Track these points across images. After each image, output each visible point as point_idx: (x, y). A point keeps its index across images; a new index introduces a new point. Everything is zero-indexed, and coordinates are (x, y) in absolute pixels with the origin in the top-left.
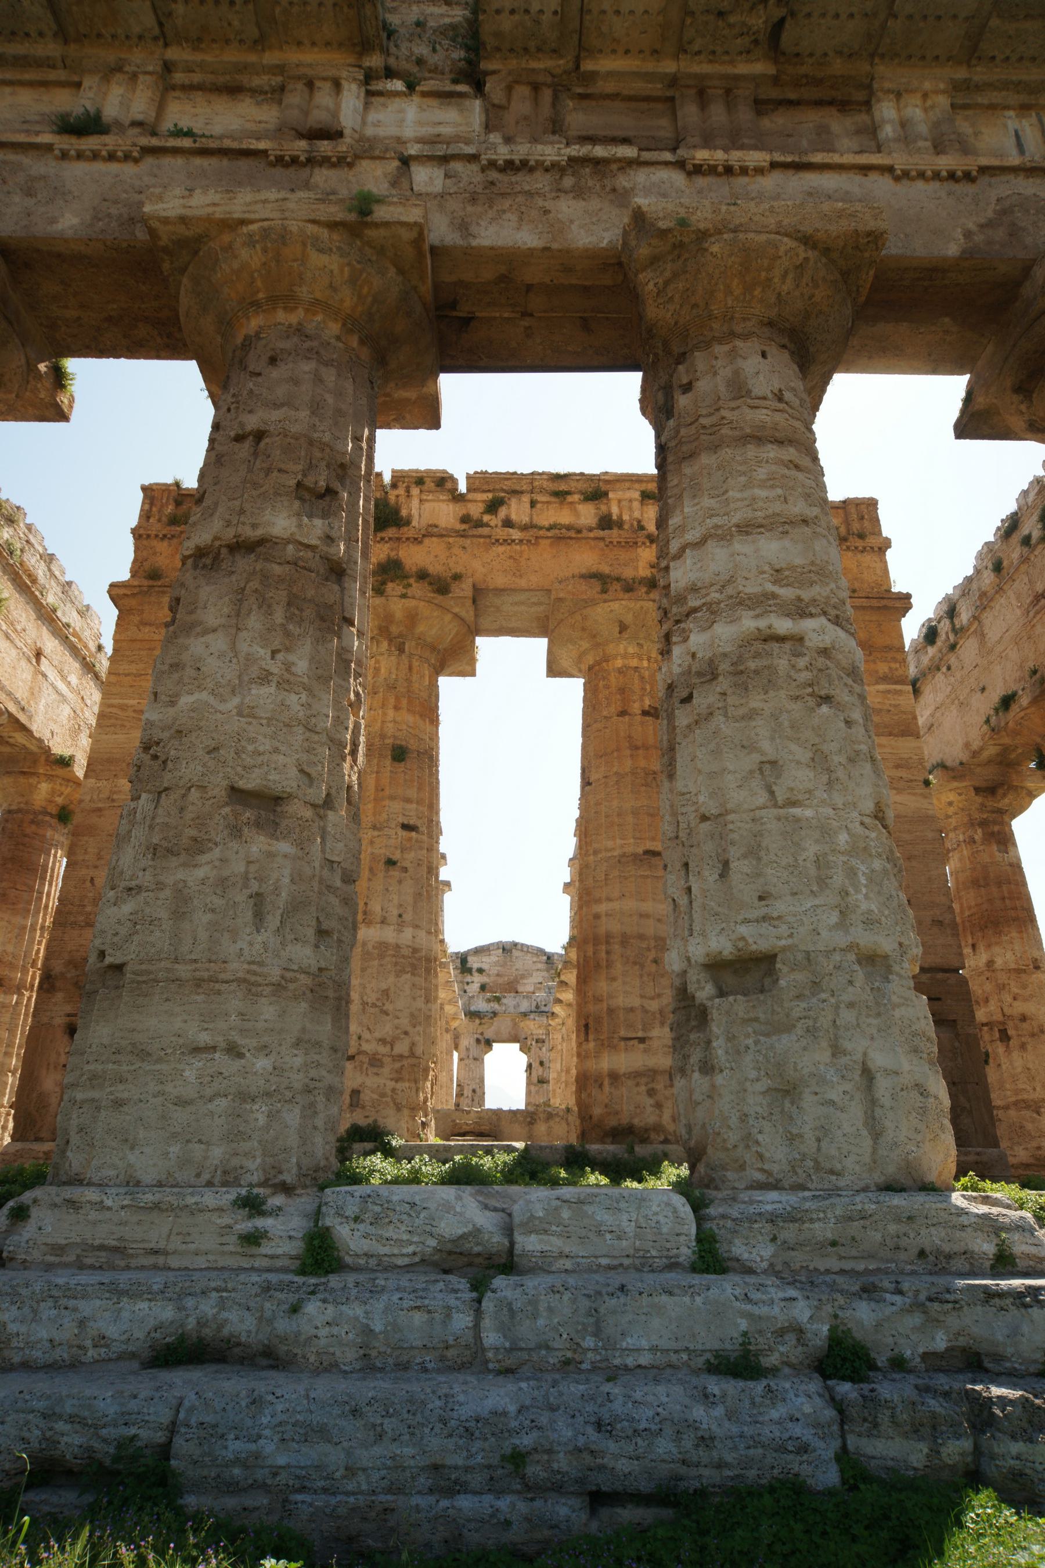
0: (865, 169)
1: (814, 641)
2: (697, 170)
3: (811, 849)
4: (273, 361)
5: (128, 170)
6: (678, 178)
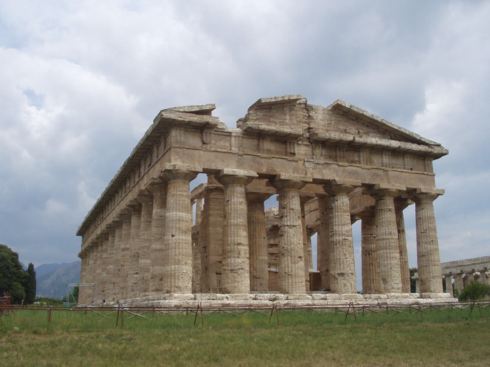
0: (358, 167)
1: (349, 240)
2: (339, 166)
3: (348, 263)
4: (293, 197)
5: (269, 160)
6: (336, 166)
